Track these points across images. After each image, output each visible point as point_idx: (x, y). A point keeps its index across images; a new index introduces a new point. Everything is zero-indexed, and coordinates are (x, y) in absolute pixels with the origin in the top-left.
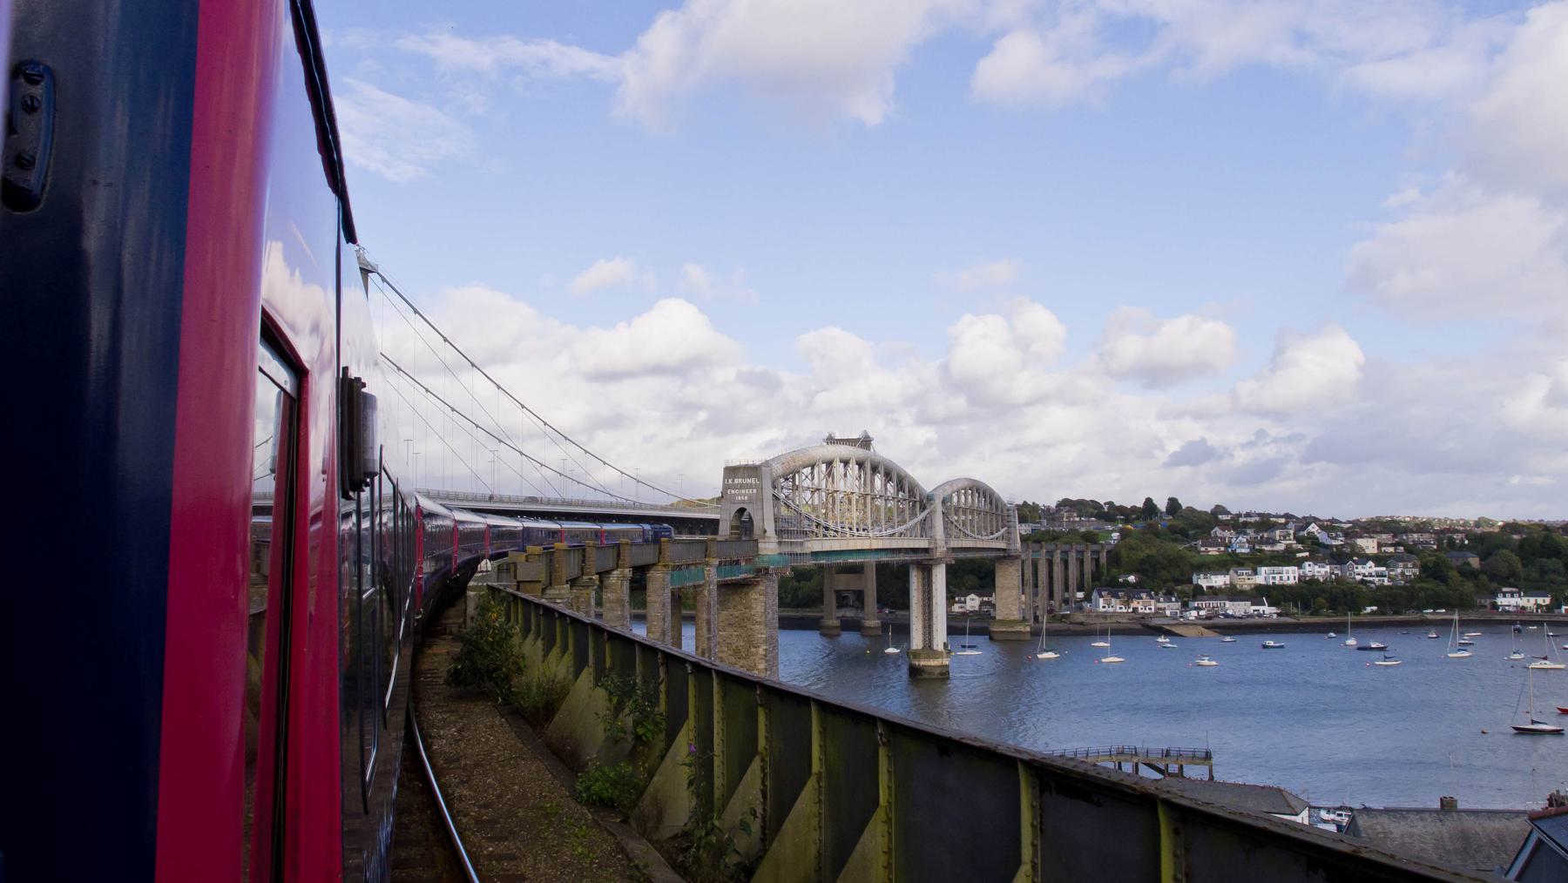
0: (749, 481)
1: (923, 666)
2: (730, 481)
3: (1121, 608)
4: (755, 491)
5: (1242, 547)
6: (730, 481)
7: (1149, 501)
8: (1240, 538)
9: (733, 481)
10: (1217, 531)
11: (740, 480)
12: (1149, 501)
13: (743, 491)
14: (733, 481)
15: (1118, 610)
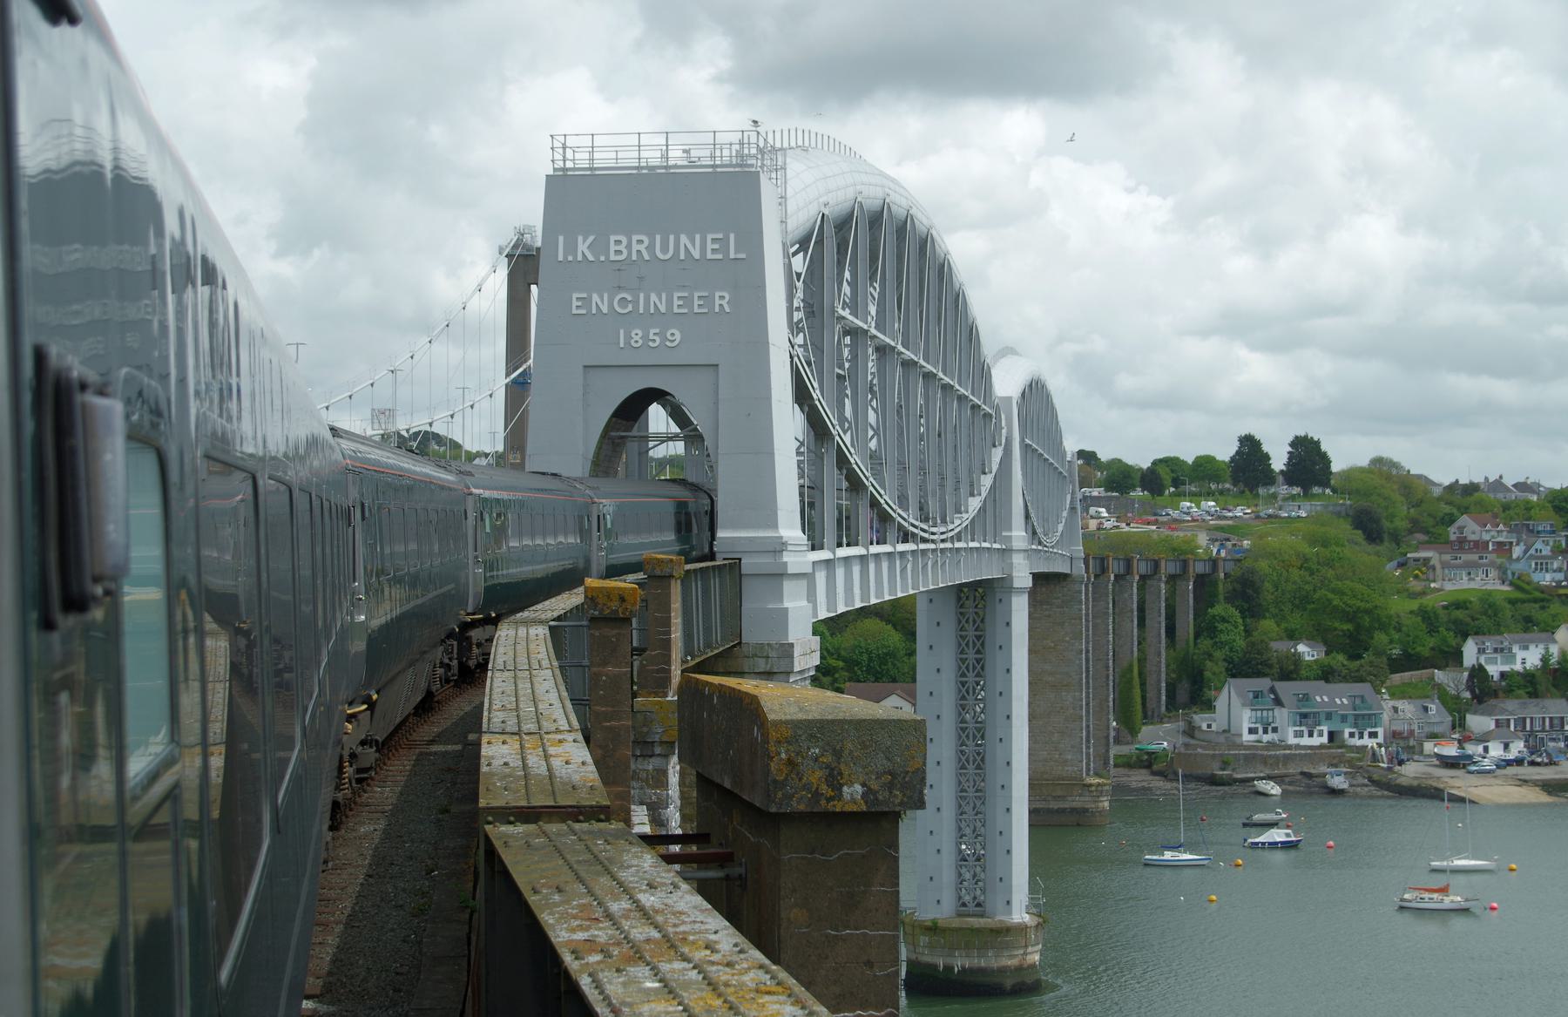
0: (690, 245)
1: (963, 970)
2: (583, 246)
3: (1299, 734)
4: (723, 299)
5: (1542, 567)
6: (583, 246)
7: (1250, 448)
8: (1538, 545)
9: (599, 246)
10: (1470, 527)
11: (640, 245)
12: (1250, 448)
13: (658, 301)
14: (599, 246)
15: (1292, 740)
